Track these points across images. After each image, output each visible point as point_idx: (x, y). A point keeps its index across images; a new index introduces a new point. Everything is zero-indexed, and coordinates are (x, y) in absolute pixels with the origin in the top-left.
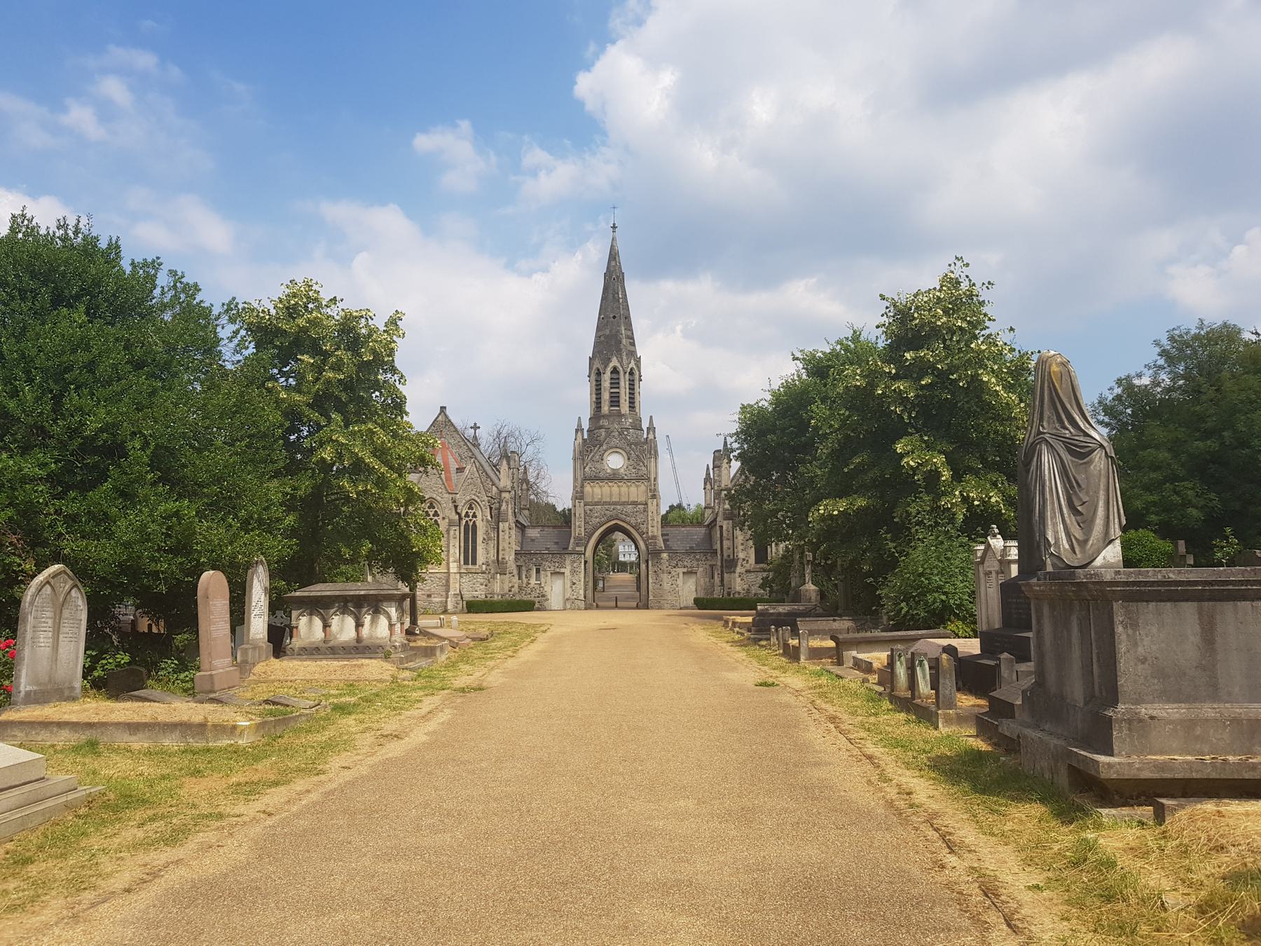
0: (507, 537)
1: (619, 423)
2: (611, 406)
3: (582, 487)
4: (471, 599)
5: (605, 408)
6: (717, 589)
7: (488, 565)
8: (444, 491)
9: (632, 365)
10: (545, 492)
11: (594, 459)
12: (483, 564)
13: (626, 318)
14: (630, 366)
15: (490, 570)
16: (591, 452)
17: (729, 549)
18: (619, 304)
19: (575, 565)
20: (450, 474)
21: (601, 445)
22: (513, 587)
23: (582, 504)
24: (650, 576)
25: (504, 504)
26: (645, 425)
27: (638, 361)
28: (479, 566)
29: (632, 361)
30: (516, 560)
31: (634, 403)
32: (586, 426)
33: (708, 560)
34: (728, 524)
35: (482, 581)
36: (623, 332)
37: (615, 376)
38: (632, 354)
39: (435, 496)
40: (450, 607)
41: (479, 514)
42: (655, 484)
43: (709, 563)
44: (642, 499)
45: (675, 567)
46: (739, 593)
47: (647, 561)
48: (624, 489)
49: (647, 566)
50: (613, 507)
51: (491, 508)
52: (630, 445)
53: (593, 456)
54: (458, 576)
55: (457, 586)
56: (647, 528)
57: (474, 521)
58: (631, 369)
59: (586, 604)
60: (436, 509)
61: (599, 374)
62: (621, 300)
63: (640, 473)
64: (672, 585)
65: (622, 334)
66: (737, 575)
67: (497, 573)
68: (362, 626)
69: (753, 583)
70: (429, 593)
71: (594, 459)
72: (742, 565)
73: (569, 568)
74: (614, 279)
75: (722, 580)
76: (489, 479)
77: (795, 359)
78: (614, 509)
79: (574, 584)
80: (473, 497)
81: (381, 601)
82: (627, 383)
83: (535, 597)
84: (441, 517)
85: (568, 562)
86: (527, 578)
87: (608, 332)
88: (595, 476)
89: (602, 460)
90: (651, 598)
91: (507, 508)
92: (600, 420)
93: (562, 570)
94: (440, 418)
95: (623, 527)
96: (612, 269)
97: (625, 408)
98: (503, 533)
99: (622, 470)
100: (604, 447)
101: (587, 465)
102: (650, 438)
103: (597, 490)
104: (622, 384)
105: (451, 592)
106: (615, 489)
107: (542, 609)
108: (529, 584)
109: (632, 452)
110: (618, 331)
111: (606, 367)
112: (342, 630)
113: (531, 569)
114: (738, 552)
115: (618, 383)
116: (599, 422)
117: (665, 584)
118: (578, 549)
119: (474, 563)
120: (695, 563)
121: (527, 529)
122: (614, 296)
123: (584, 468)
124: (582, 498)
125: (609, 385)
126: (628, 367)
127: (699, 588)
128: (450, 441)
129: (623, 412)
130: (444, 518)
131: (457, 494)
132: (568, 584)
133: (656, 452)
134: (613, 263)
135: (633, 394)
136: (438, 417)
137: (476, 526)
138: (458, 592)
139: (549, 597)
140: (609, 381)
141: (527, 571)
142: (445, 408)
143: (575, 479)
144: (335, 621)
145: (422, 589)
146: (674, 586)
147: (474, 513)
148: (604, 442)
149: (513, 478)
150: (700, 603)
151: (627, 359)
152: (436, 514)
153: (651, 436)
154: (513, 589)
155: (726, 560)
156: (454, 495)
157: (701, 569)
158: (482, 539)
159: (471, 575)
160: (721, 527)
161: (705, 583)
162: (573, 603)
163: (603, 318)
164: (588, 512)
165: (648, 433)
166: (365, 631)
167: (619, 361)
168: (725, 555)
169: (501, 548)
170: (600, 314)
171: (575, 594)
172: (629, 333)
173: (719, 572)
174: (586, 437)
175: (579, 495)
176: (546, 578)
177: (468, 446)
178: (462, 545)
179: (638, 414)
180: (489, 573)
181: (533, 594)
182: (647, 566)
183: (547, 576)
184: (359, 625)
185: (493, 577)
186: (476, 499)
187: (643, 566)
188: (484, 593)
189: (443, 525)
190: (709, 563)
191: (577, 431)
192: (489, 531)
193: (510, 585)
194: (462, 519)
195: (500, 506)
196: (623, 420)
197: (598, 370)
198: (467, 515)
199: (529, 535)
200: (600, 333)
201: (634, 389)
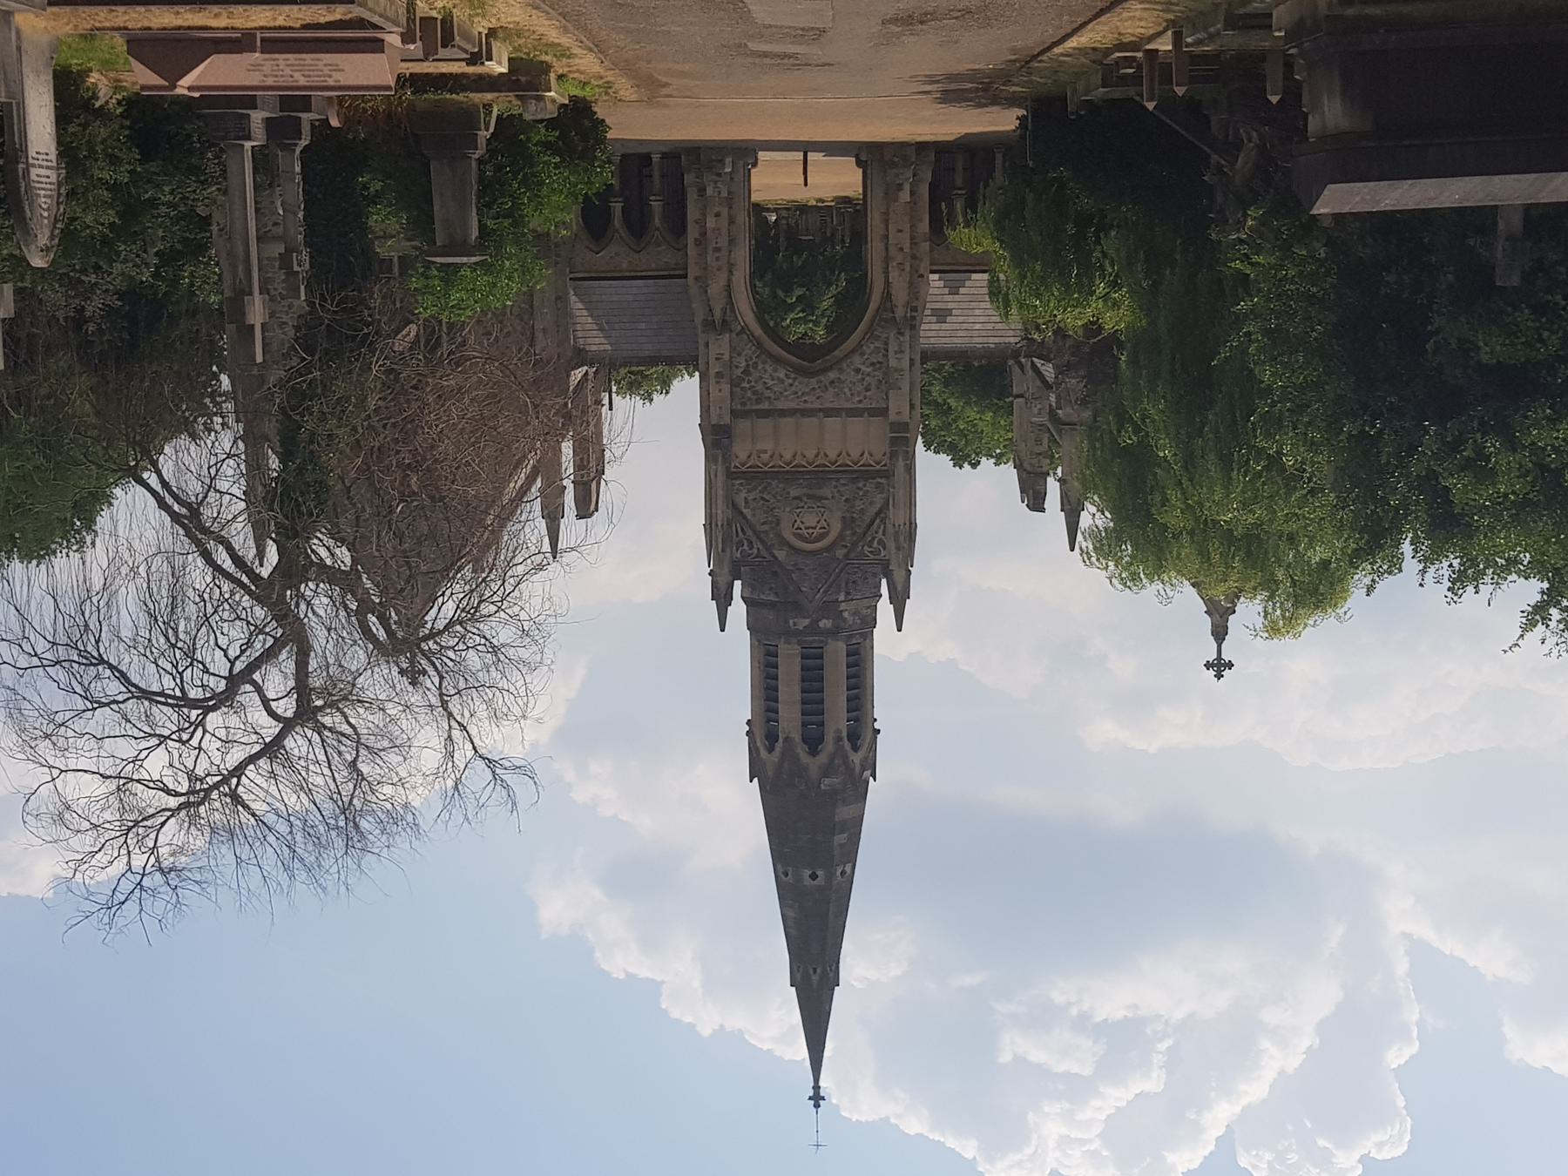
32: (885, 609)
44: (743, 425)
58: (771, 749)
61: (854, 737)
74: (815, 971)
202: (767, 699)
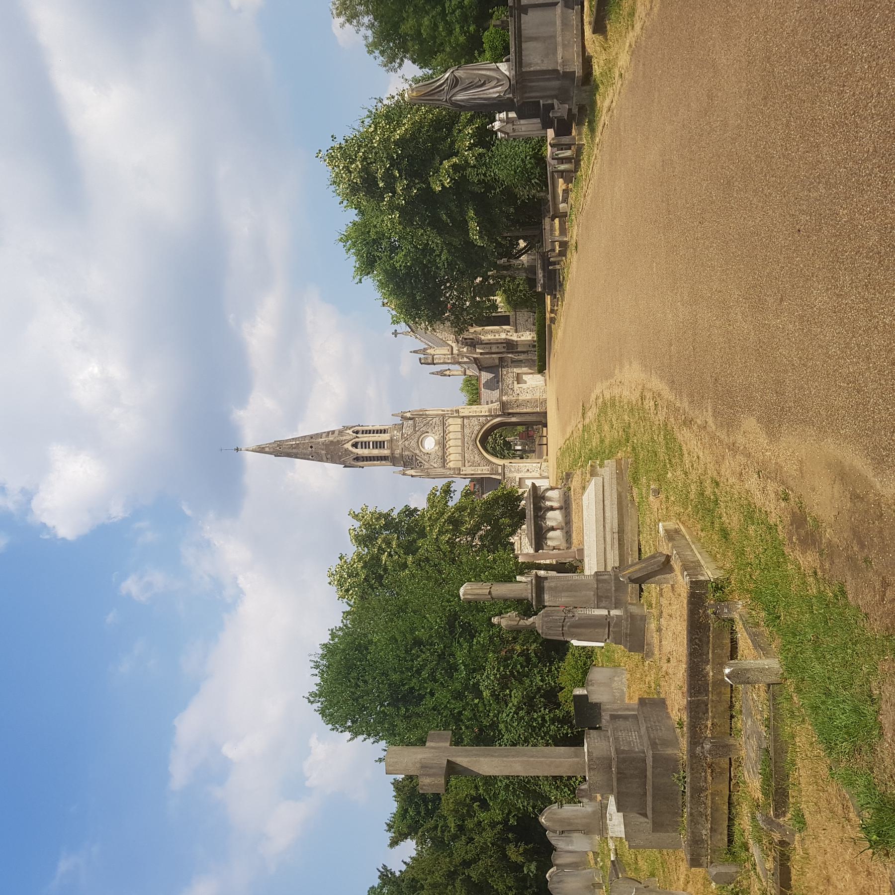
1: (397, 441)
2: (384, 447)
3: (450, 469)
5: (386, 452)
9: (350, 432)
11: (427, 460)
13: (312, 438)
14: (351, 433)
17: (498, 347)
19: (513, 470)
21: (416, 454)
23: (464, 468)
24: (522, 411)
29: (347, 432)
34: (478, 348)
37: (359, 446)
38: (341, 432)
43: (510, 364)
45: (514, 391)
46: (533, 337)
47: (509, 414)
50: (466, 444)
53: (425, 461)
62: (297, 442)
66: (519, 339)
68: (552, 506)
71: (427, 460)
72: (511, 336)
73: (515, 474)
75: (523, 352)
77: (360, 281)
78: (468, 443)
79: (528, 470)
81: (537, 495)
85: (511, 475)
87: (324, 452)
89: (427, 454)
90: (538, 410)
92: (395, 457)
93: (517, 480)
96: (272, 450)
97: (385, 437)
99: (436, 437)
100: (417, 452)
101: (432, 465)
110: (323, 443)
111: (352, 453)
112: (555, 519)
114: (501, 339)
115: (365, 442)
116: (397, 458)
118: (500, 471)
120: (510, 375)
122: (295, 448)
123: (435, 468)
125: (367, 450)
129: (389, 438)
133: (421, 411)
134: (267, 449)
135: (374, 431)
140: (364, 450)
144: (550, 523)
146: (528, 391)
148: (413, 452)
150: (541, 369)
155: (507, 349)
157: (515, 370)
159: (523, 548)
160: (481, 354)
161: (526, 367)
163: (312, 457)
164: (470, 464)
166: (555, 504)
167: (348, 442)
170: (309, 459)
172: (324, 435)
173: (517, 354)
182: (513, 414)
184: (552, 509)
187: (514, 419)
190: (510, 364)
196: (395, 438)
197: (354, 459)
200: (324, 458)
201: (370, 431)
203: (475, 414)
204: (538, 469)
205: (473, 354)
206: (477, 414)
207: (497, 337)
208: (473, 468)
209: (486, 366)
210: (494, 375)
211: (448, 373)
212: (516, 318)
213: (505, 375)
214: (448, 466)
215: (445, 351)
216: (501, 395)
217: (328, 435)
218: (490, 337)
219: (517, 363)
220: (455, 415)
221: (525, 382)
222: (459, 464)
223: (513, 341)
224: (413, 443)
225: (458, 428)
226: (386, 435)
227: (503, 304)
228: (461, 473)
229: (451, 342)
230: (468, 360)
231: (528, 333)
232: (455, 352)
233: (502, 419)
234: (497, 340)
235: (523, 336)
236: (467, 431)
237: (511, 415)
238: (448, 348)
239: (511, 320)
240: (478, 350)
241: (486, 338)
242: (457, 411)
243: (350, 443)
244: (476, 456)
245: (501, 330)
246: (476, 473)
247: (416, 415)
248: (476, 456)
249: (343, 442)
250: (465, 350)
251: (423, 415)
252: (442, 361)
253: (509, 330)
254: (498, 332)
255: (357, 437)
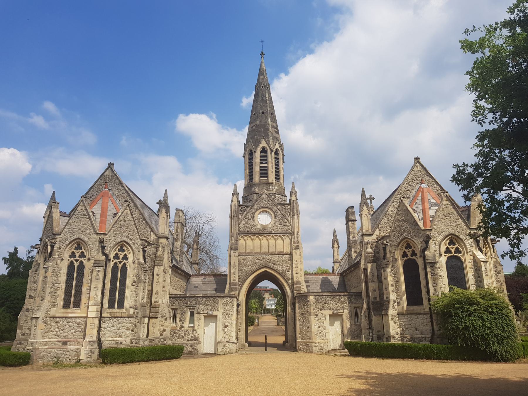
0: (161, 280)
1: (268, 189)
2: (261, 177)
3: (237, 240)
4: (112, 346)
5: (257, 178)
6: (365, 332)
7: (136, 309)
8: (93, 232)
9: (277, 146)
10: (216, 256)
11: (247, 217)
12: (131, 308)
15: (138, 313)
16: (244, 211)
17: (375, 290)
18: (267, 103)
19: (227, 307)
20: (106, 218)
22: (164, 330)
23: (237, 254)
24: (297, 319)
25: (161, 249)
26: (288, 194)
27: (281, 146)
28: (126, 309)
29: (277, 144)
30: (171, 303)
31: (279, 176)
32: (241, 193)
33: (352, 303)
34: (372, 266)
35: (129, 325)
36: (270, 123)
37: (263, 154)
38: (277, 139)
39: (82, 237)
40: (83, 356)
41: (131, 257)
42: (298, 238)
43: (354, 305)
45: (321, 310)
46: (394, 337)
47: (294, 304)
48: (272, 241)
49: (294, 309)
50: (262, 257)
51: (144, 252)
52: (276, 205)
53: (246, 214)
54: (96, 321)
55: (95, 332)
56: (292, 275)
57: (125, 264)
58: (277, 150)
59: (237, 347)
60: (83, 250)
61: (251, 154)
62: (268, 102)
63: (285, 228)
64: (319, 327)
65: (269, 124)
66: (390, 318)
67: (145, 317)
69: (406, 326)
70: (65, 340)
71: (247, 217)
72: (394, 308)
75: (370, 323)
76: (148, 227)
78: (263, 259)
79: (226, 326)
80: (125, 239)
82: (274, 160)
83: (188, 340)
84: (86, 258)
86: (181, 321)
87: (258, 123)
88: (248, 231)
89: (254, 217)
91: (163, 253)
93: (215, 313)
94: (107, 173)
95: (271, 273)
96: (261, 81)
97: (272, 178)
98: (157, 277)
99: (270, 226)
100: (256, 207)
101: (241, 221)
102: (292, 200)
103: (249, 242)
104: (269, 159)
105: (88, 339)
106: (264, 241)
107: (193, 354)
108: (183, 327)
109: (278, 211)
110: (266, 122)
111: (257, 147)
113: (185, 313)
114: (388, 293)
115: (267, 160)
117: (313, 326)
118: (232, 293)
119: (121, 305)
121: (191, 278)
122: (262, 99)
123: (239, 224)
124: (236, 249)
126: (274, 148)
127: (346, 331)
128: (115, 193)
129: (270, 181)
130: (89, 259)
131: (106, 234)
132: (220, 326)
133: (298, 211)
134: (262, 77)
135: (278, 169)
136: (105, 171)
137: (126, 268)
138: (95, 338)
139: (201, 340)
141: (182, 314)
142: (113, 164)
143: (231, 233)
145: (58, 336)
147: (125, 255)
149: (177, 231)
151: (273, 142)
152: (82, 255)
153: (293, 198)
154: (164, 333)
155: (373, 302)
156: (102, 236)
158: (131, 282)
159: (115, 320)
160: (365, 270)
161: (351, 325)
162: (224, 346)
164: (242, 261)
165: (291, 196)
167: (267, 143)
168: (372, 299)
169: (154, 291)
170: (252, 112)
171: (227, 336)
172: (275, 125)
173: (367, 314)
174: (241, 203)
175: (234, 247)
176: (199, 320)
177: (131, 197)
178: (108, 286)
179: (282, 184)
180: (137, 317)
181: (187, 337)
182: (294, 309)
183: (200, 319)
185: (140, 322)
186: (129, 241)
187: (289, 309)
188: (129, 338)
189: (88, 265)
190: (354, 305)
191: (233, 194)
192: (140, 273)
193: (162, 329)
194: (110, 260)
195: (157, 251)
196: (271, 187)
198: (116, 257)
199: (193, 283)
200: (252, 125)
201: (278, 165)
202: (278, 172)
203: (294, 266)
204: (227, 340)
205: (365, 260)
206: (294, 269)
207: (391, 289)
208: (237, 264)
209: (346, 280)
210: (337, 288)
211: (336, 245)
212: (420, 314)
213: (339, 299)
214: (240, 238)
215: (367, 227)
216: (316, 295)
217: (273, 127)
218: (390, 279)
219: (355, 315)
220: (294, 246)
221: (332, 324)
222: (241, 250)
223: (387, 309)
224: (264, 203)
225: (280, 249)
226: (274, 179)
227: (440, 295)
228: (232, 251)
229: (378, 234)
230: (353, 258)
231: (398, 330)
232: (366, 239)
233: (290, 296)
234: (387, 289)
235: (395, 323)
236: (277, 258)
237: (292, 306)
238: (370, 231)
239: (416, 307)
240: (369, 266)
241: (389, 274)
242: (297, 248)
243: (266, 146)
244: (250, 267)
245: (401, 294)
246: (232, 268)
247: (294, 206)
248: (250, 267)
249: (267, 140)
250: (369, 250)
251: (293, 212)
252: (351, 230)
253: (401, 305)
254: (397, 290)
255: (272, 151)
